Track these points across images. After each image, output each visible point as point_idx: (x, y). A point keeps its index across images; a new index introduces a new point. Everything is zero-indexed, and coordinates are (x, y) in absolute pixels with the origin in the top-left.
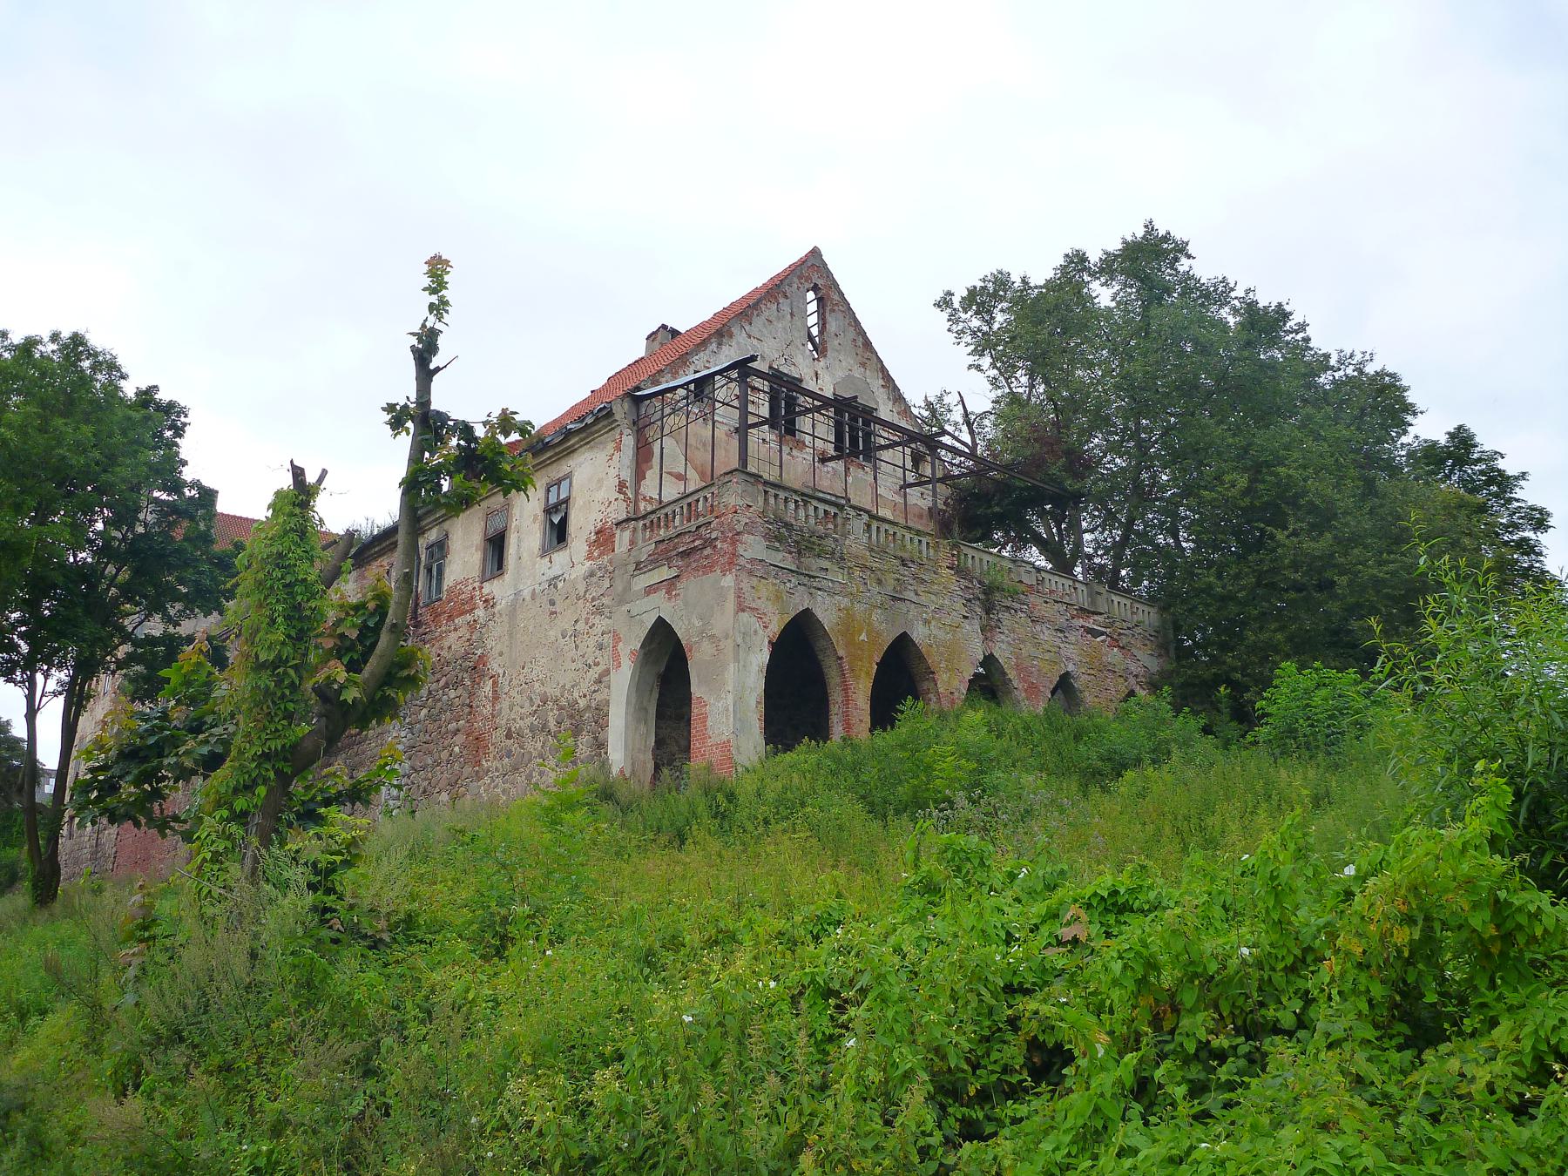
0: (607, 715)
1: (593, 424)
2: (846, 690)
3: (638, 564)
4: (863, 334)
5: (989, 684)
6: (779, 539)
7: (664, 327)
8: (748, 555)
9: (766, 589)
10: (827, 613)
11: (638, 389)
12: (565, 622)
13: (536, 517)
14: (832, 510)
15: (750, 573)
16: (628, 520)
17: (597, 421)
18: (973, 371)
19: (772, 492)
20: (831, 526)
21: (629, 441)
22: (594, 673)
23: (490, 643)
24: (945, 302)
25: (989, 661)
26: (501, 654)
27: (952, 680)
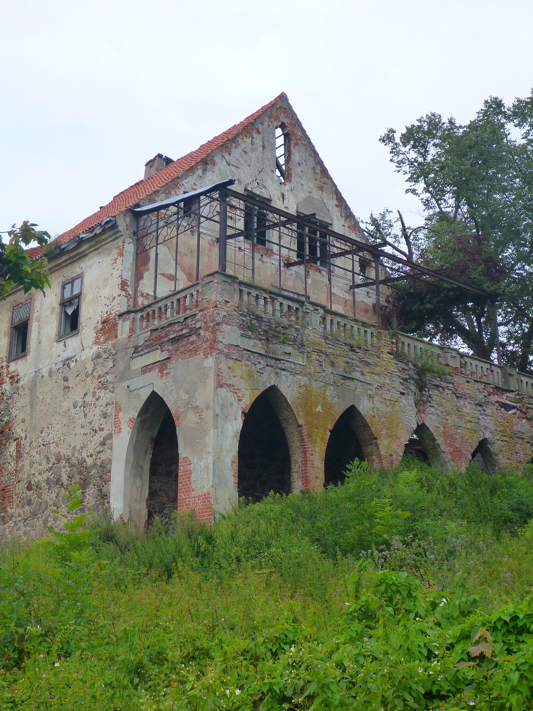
0: (109, 471)
1: (101, 234)
2: (304, 452)
3: (136, 348)
4: (320, 163)
5: (421, 448)
6: (250, 328)
7: (160, 156)
8: (226, 341)
9: (240, 369)
10: (289, 389)
11: (138, 206)
12: (76, 395)
14: (295, 305)
15: (228, 356)
16: (128, 312)
17: (104, 231)
18: (410, 194)
19: (246, 290)
20: (293, 318)
21: (130, 248)
22: (99, 437)
23: (14, 412)
24: (388, 138)
25: (421, 429)
26: (23, 421)
27: (391, 445)
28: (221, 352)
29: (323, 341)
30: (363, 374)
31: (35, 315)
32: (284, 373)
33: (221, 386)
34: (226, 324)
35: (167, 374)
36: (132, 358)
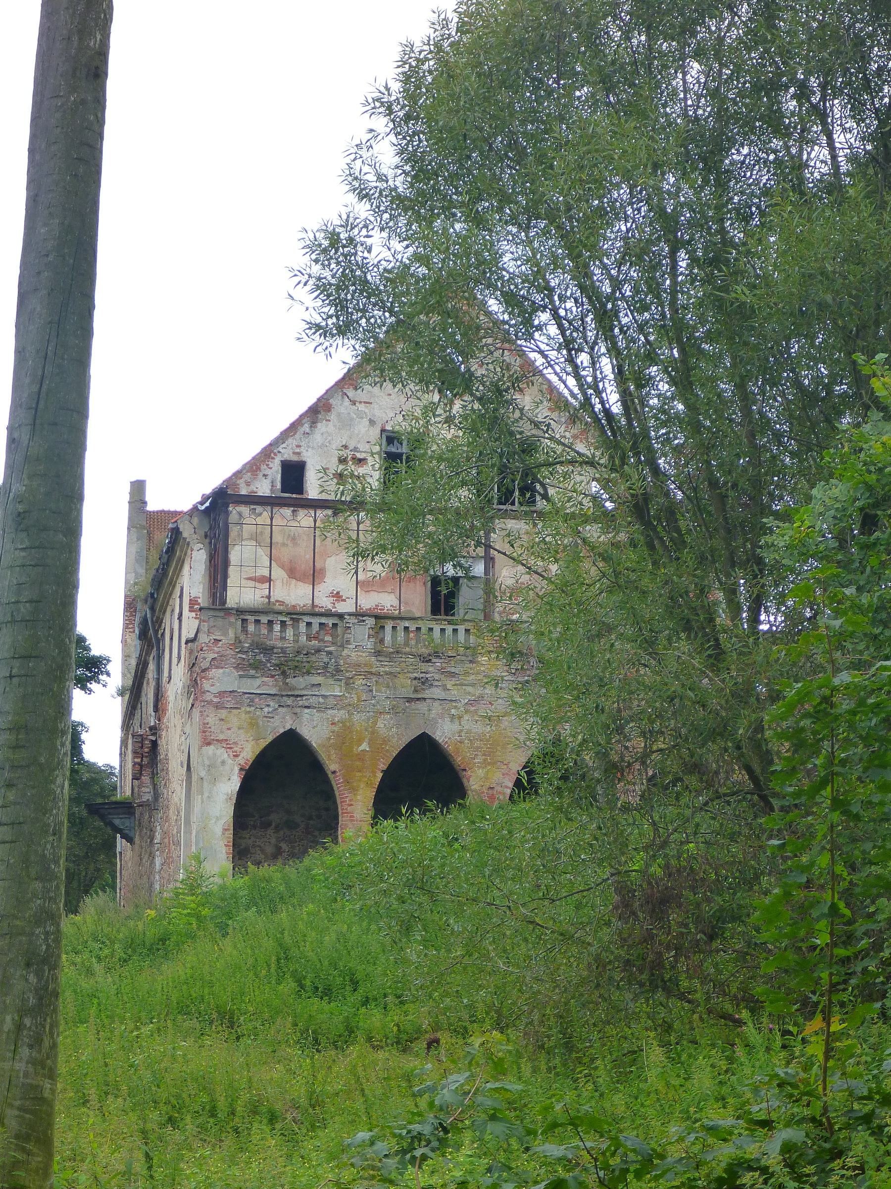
6: (257, 666)
8: (214, 690)
9: (237, 719)
10: (315, 730)
14: (330, 622)
15: (218, 707)
19: (251, 618)
28: (210, 703)
29: (373, 659)
30: (445, 688)
32: (306, 711)
33: (209, 744)
34: (217, 667)
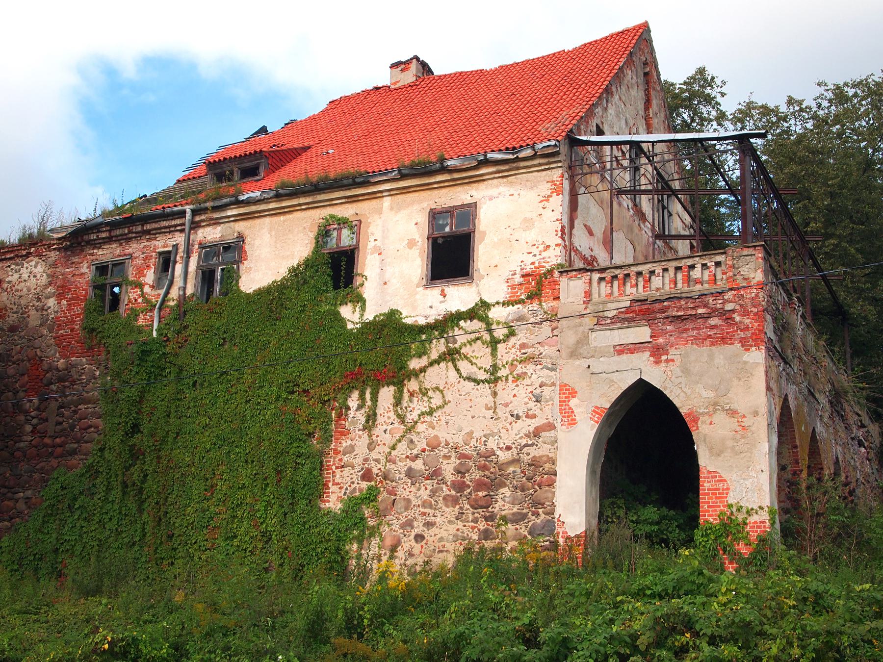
13: (411, 244)
22: (526, 426)
31: (371, 245)
35: (667, 361)
36: (592, 330)
